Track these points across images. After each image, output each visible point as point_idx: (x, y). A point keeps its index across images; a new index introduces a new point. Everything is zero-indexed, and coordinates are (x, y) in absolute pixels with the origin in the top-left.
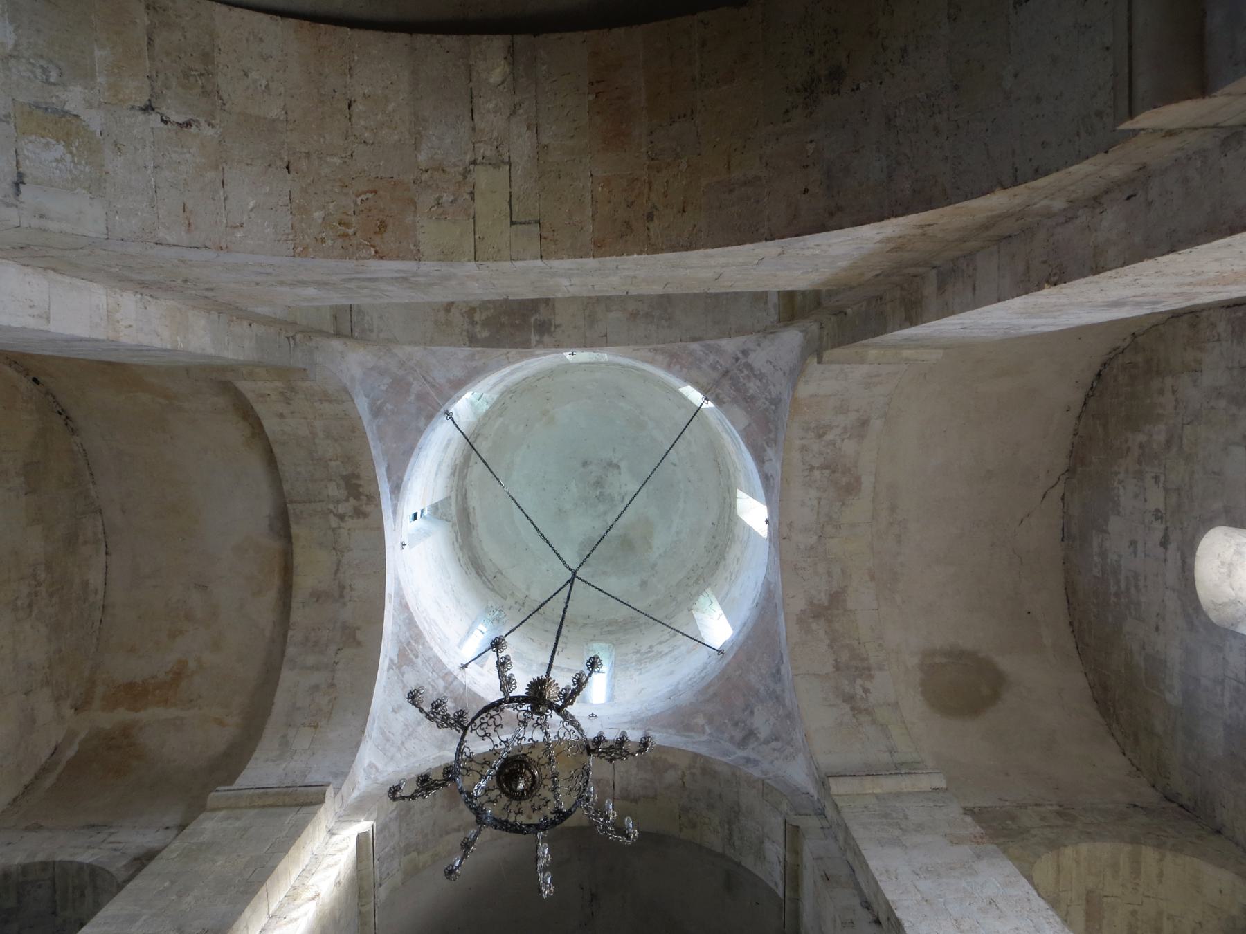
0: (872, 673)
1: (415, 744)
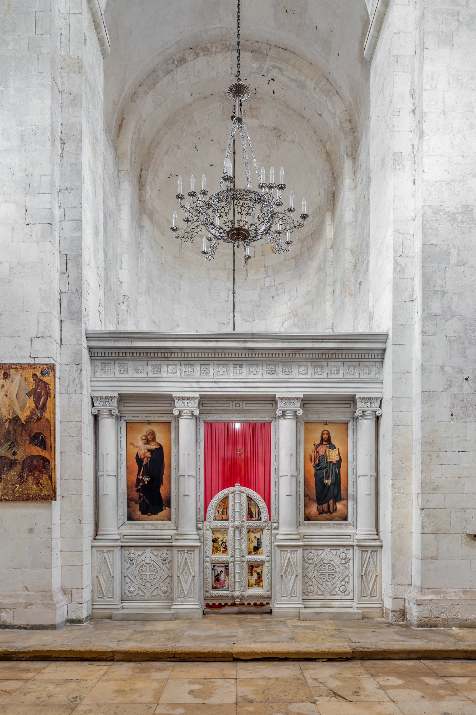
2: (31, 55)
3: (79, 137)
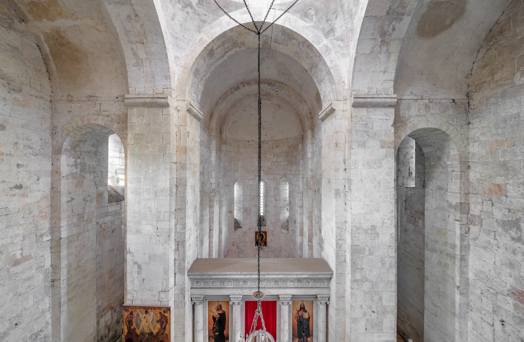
0: (403, 17)
1: (188, 34)
3: (185, 184)
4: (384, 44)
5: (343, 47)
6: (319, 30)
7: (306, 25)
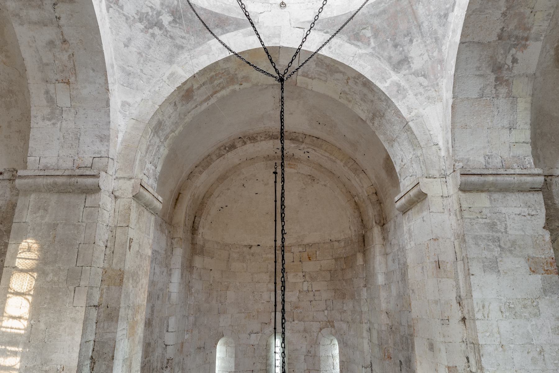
0: (528, 43)
1: (151, 66)
2: (68, 287)
3: (111, 355)
4: (501, 84)
5: (428, 86)
6: (382, 59)
7: (358, 52)
